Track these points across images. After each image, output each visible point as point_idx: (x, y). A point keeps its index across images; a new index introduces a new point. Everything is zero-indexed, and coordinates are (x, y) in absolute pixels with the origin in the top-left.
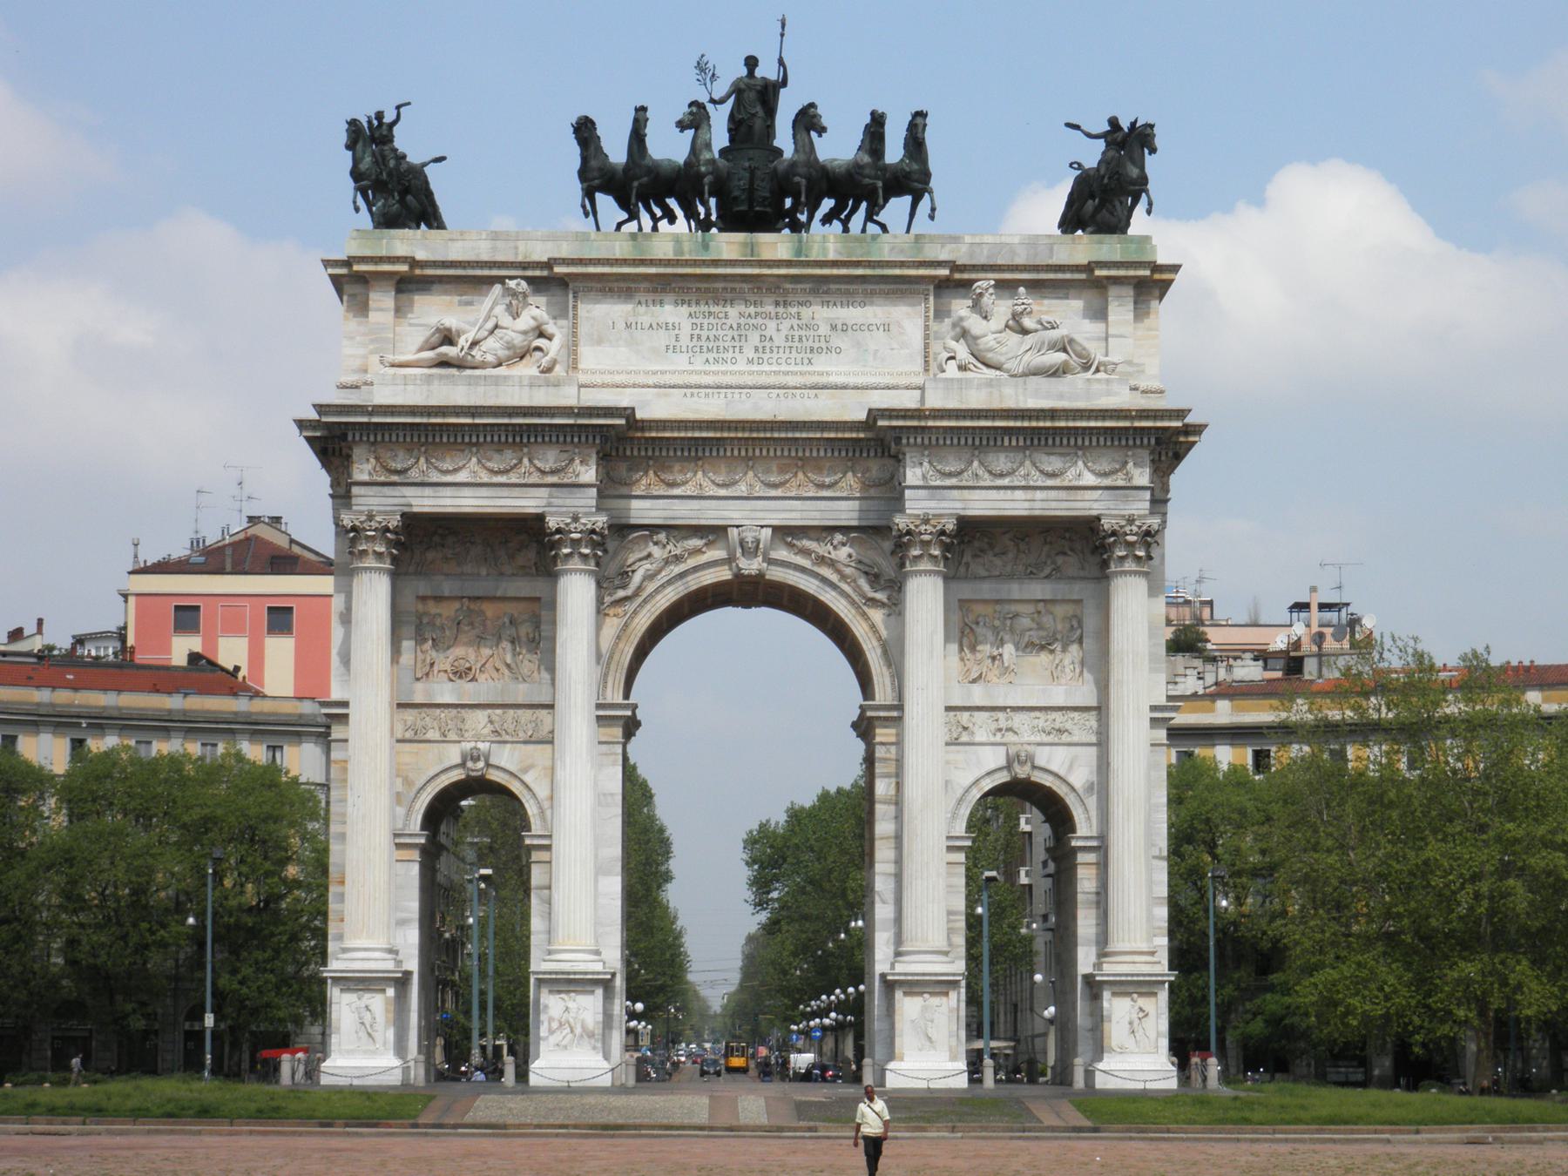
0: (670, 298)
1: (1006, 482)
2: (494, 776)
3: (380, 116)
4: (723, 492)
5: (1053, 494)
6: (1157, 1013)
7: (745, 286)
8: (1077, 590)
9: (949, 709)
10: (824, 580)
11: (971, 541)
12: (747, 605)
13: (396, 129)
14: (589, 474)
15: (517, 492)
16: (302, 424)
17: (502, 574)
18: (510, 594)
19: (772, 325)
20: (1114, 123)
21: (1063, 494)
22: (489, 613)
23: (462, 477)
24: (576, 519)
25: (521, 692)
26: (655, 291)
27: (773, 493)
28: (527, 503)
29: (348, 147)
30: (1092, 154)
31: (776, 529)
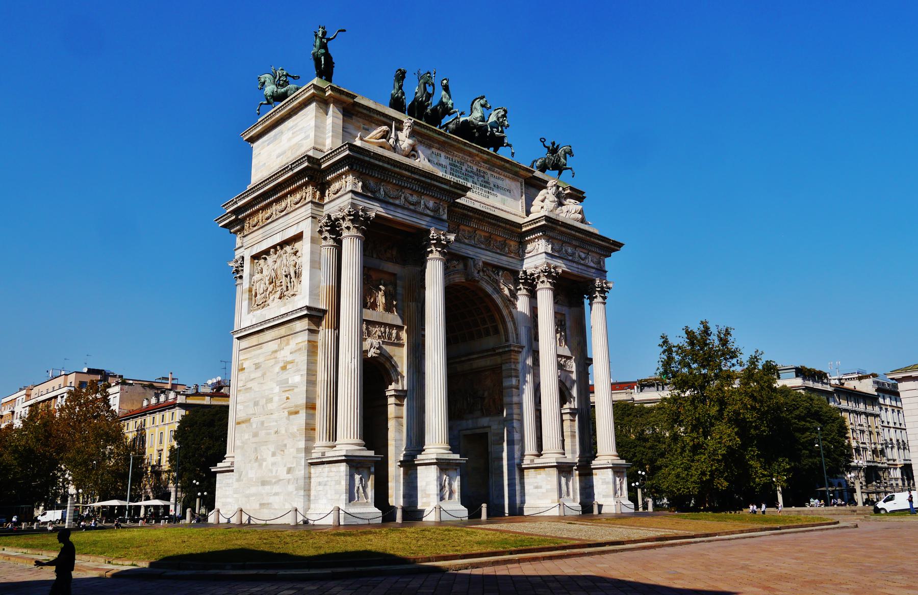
0: (443, 154)
1: (570, 258)
4: (466, 241)
5: (583, 268)
7: (470, 159)
10: (495, 289)
14: (445, 217)
17: (380, 259)
18: (385, 269)
19: (476, 178)
20: (553, 144)
21: (585, 268)
22: (373, 277)
23: (397, 202)
26: (439, 149)
27: (483, 246)
28: (423, 223)
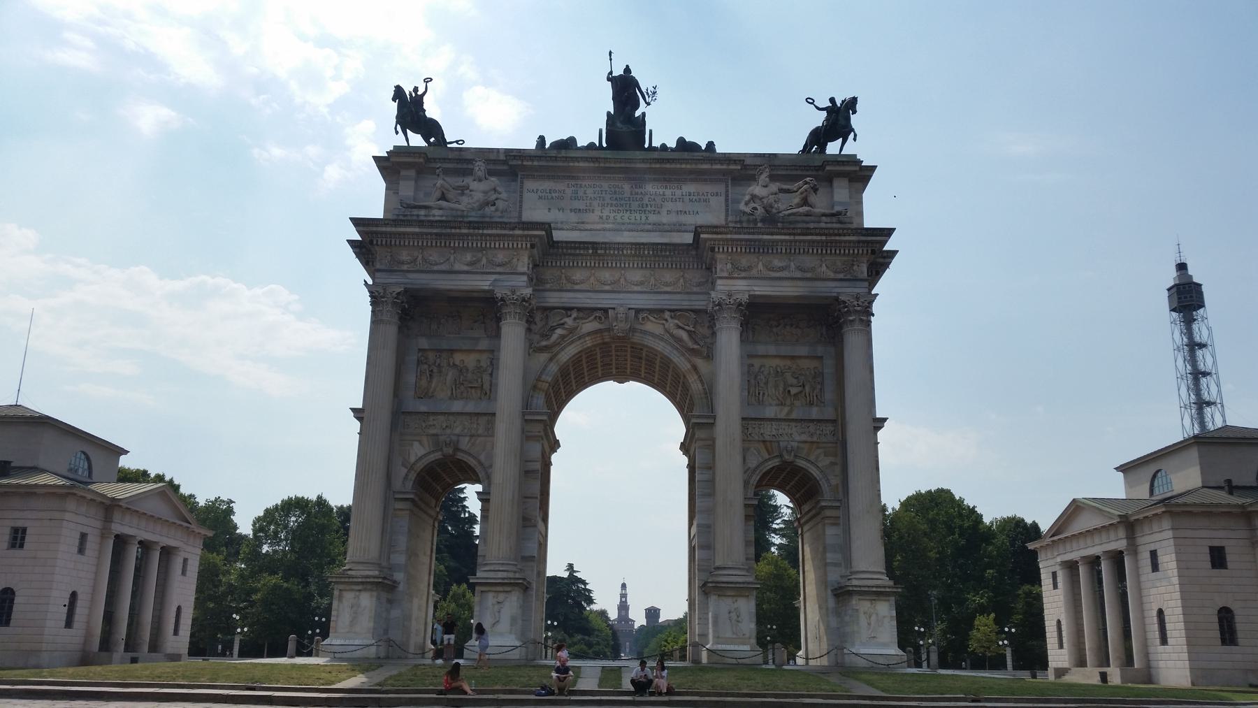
2: (460, 456)
3: (416, 89)
6: (885, 611)
8: (820, 350)
9: (743, 419)
11: (757, 315)
12: (621, 381)
13: (425, 99)
15: (478, 277)
16: (351, 242)
20: (832, 100)
24: (513, 292)
25: (483, 407)
27: (636, 288)
29: (394, 100)
30: (819, 119)
31: (638, 311)
